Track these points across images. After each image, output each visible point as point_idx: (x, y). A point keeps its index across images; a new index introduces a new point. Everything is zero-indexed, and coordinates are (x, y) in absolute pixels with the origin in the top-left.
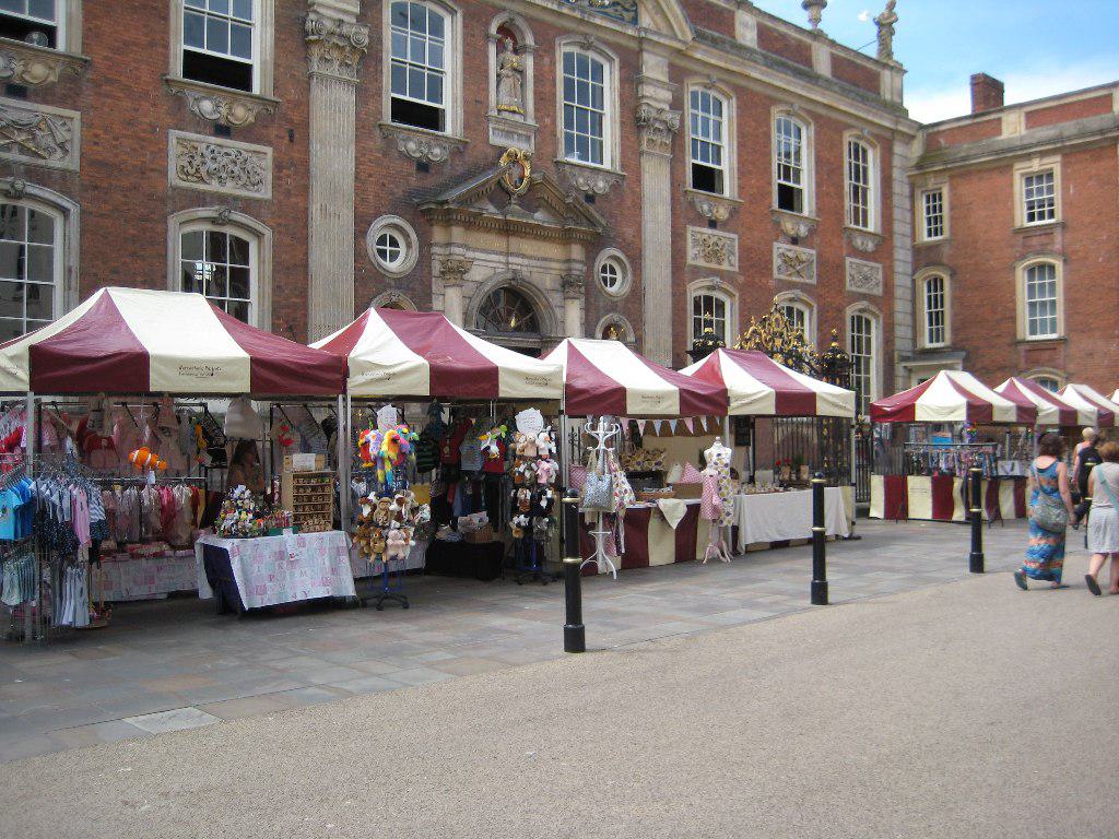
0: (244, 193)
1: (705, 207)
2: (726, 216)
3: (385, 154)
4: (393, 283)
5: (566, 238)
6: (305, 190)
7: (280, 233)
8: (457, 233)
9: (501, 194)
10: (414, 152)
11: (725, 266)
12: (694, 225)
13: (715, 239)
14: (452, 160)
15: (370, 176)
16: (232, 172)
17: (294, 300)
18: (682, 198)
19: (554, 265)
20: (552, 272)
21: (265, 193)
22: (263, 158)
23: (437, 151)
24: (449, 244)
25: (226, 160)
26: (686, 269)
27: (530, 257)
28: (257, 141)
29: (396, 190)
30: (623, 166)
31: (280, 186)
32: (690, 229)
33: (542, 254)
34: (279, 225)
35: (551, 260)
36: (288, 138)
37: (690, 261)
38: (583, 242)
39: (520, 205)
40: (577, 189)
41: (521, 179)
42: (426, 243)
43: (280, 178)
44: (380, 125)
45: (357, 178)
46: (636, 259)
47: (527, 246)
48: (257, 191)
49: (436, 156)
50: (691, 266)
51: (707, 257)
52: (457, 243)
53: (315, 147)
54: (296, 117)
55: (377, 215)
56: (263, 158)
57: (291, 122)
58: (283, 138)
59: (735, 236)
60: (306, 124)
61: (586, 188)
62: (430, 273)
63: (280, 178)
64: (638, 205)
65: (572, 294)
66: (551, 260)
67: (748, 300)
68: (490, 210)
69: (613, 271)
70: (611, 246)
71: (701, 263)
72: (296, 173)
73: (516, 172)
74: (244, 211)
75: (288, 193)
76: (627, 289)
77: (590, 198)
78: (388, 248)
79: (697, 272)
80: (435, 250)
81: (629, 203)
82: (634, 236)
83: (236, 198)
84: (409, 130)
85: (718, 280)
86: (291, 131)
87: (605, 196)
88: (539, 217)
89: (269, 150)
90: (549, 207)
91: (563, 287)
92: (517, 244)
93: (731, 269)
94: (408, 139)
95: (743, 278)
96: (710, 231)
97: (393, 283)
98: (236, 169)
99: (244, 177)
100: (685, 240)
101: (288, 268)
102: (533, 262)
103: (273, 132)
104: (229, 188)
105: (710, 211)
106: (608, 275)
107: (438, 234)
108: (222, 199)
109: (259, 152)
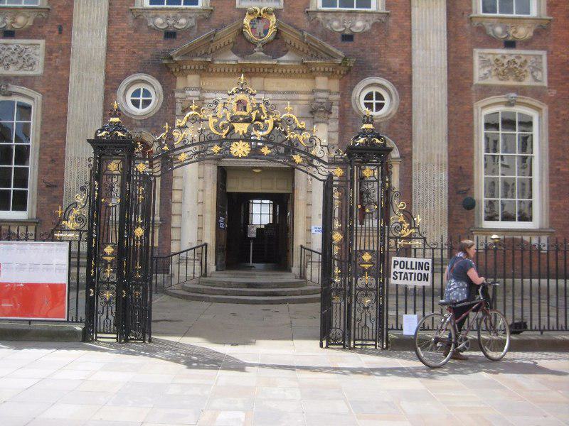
0: (22, 73)
1: (499, 30)
2: (531, 34)
3: (136, 31)
4: (139, 123)
5: (308, 71)
6: (67, 65)
7: (48, 96)
8: (193, 79)
9: (242, 44)
10: (161, 25)
11: (528, 82)
12: (483, 48)
13: (513, 57)
14: (198, 26)
15: (122, 48)
16: (12, 60)
17: (58, 141)
18: (467, 25)
19: (301, 97)
20: (300, 102)
21: (38, 70)
22: (37, 49)
23: (183, 21)
24: (183, 91)
25: (8, 53)
26: (473, 89)
27: (273, 92)
28: (35, 37)
29: (144, 55)
30: (388, 6)
31: (50, 64)
32: (477, 52)
33: (289, 88)
34: (48, 91)
35: (298, 93)
36: (57, 32)
37: (477, 81)
38: (330, 74)
39: (263, 52)
40: (333, 32)
41: (266, 32)
42: (169, 91)
43: (50, 59)
44: (131, 10)
45: (109, 49)
46: (404, 86)
47: (272, 83)
48: (31, 70)
49: (182, 25)
50: (479, 85)
51: (502, 75)
52: (189, 86)
53: (75, 33)
54: (65, 17)
55: (127, 74)
56: (37, 49)
57: (61, 20)
58: (54, 32)
59: (544, 53)
60: (70, 21)
61: (342, 29)
62: (174, 113)
63: (50, 59)
64: (407, 37)
65: (317, 119)
66: (298, 93)
67: (562, 112)
68: (232, 58)
69: (379, 96)
70: (373, 75)
71: (493, 81)
72: (63, 54)
73: (260, 26)
74: (22, 84)
75: (57, 68)
76: (393, 110)
77: (348, 38)
78: (141, 98)
79: (486, 91)
80: (177, 95)
81: (395, 36)
82: (402, 65)
83: (17, 77)
84: (156, 9)
85: (513, 95)
86: (61, 26)
87: (365, 34)
88: (286, 59)
89: (42, 42)
90: (296, 50)
91: (313, 112)
92: (257, 82)
93: (538, 84)
94: (156, 16)
95: (554, 92)
96: (504, 51)
97: (139, 123)
98: (15, 58)
99: (21, 61)
100: (472, 63)
101: (53, 120)
102: (279, 96)
103: (47, 29)
104: (13, 71)
105: (505, 32)
106: (374, 101)
107: (180, 83)
108: (7, 79)
109: (34, 45)
